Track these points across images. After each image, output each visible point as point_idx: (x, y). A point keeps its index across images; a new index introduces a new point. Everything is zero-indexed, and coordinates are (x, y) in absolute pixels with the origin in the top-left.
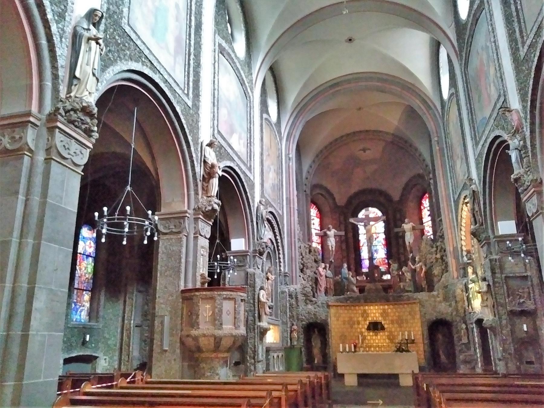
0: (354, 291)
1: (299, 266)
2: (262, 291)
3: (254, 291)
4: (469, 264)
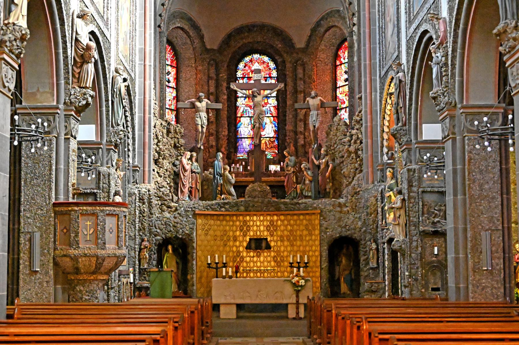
0: (230, 194)
1: (154, 156)
3: (109, 196)
4: (389, 165)
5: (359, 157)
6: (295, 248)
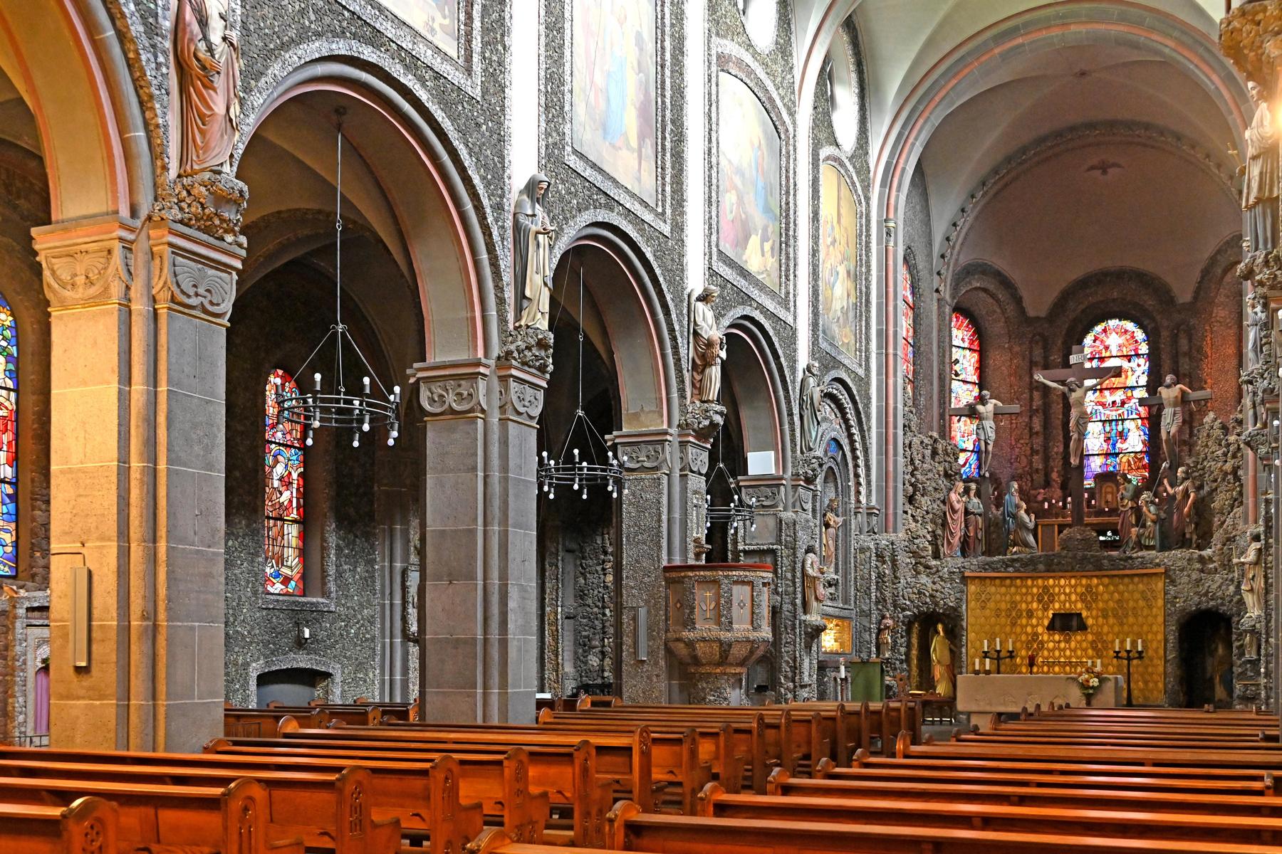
0: (1026, 545)
2: (811, 555)
3: (794, 554)
5: (1239, 480)
6: (1126, 627)
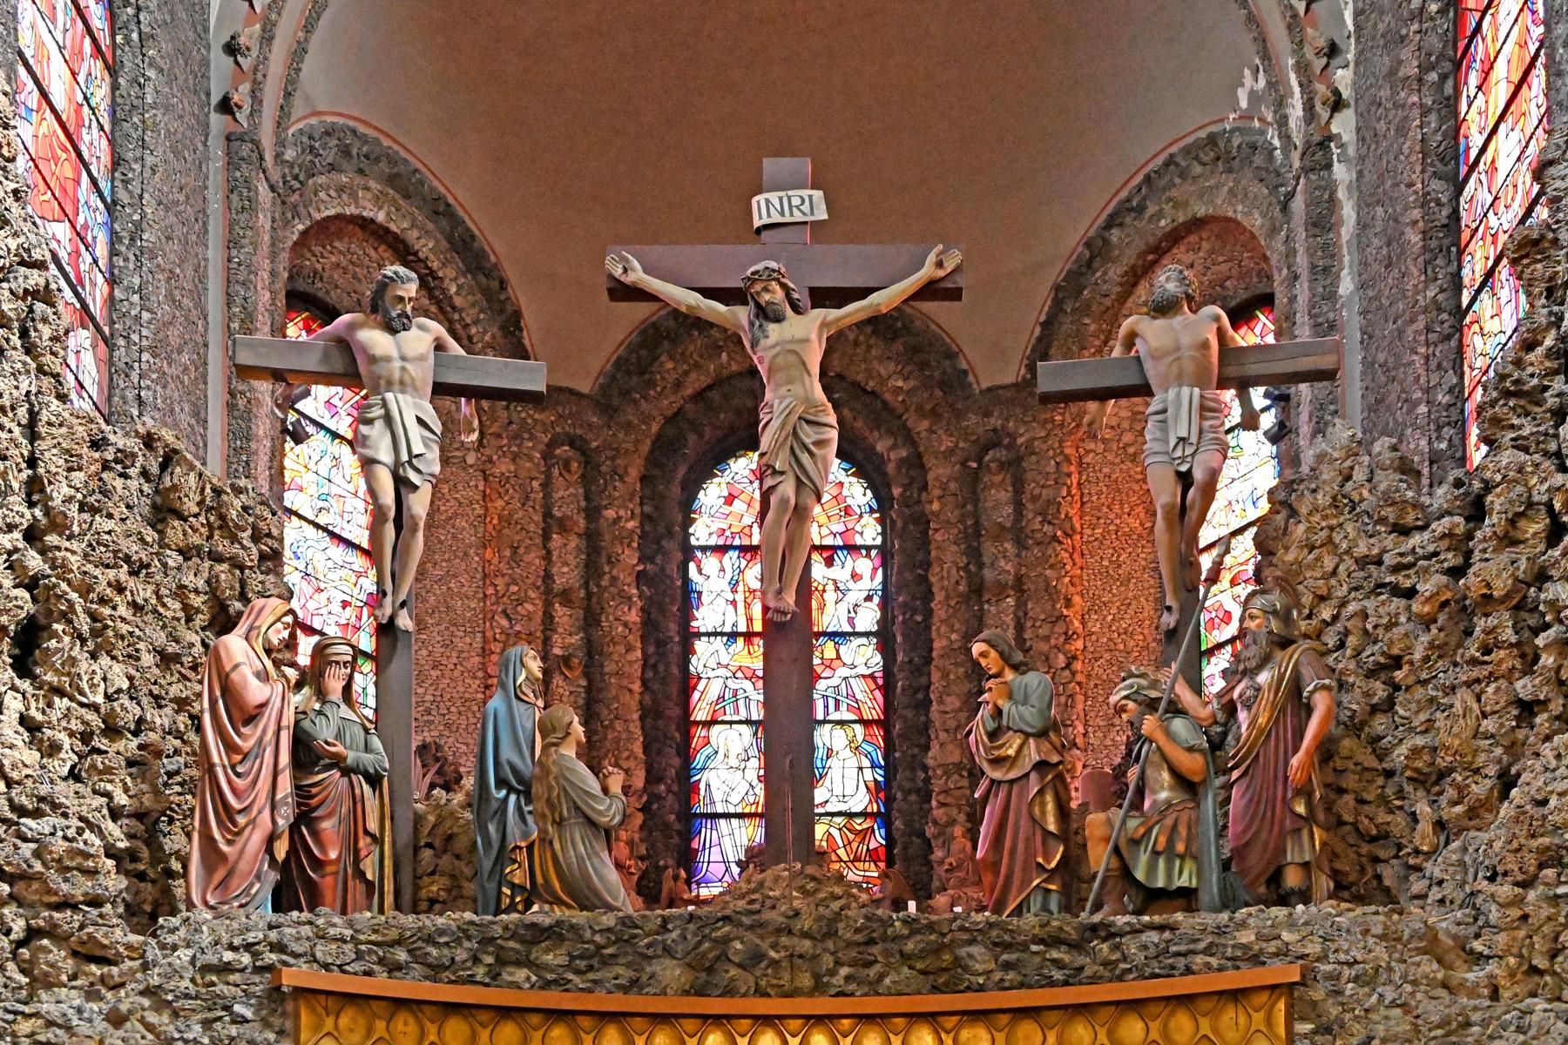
0: (586, 897)
